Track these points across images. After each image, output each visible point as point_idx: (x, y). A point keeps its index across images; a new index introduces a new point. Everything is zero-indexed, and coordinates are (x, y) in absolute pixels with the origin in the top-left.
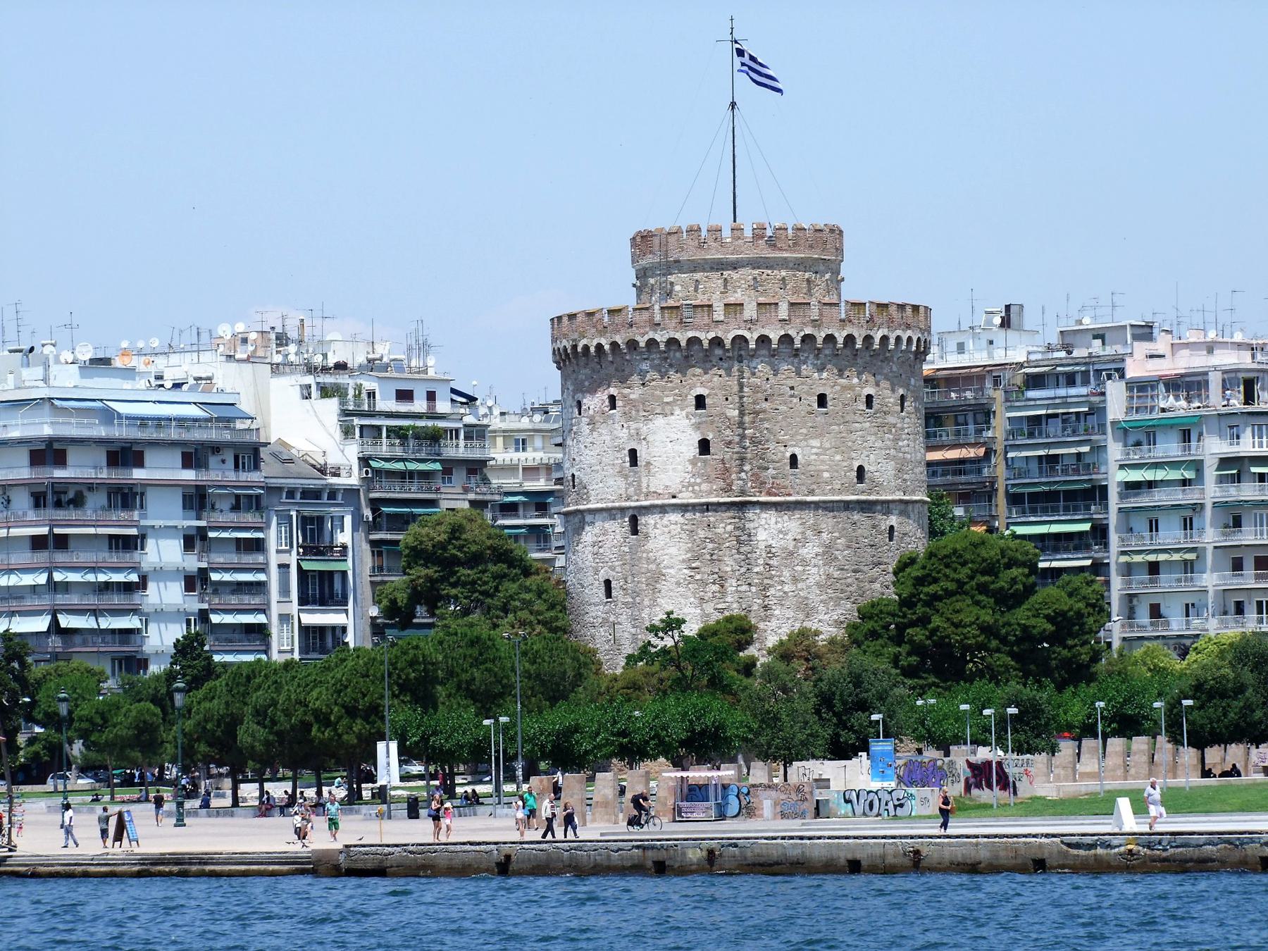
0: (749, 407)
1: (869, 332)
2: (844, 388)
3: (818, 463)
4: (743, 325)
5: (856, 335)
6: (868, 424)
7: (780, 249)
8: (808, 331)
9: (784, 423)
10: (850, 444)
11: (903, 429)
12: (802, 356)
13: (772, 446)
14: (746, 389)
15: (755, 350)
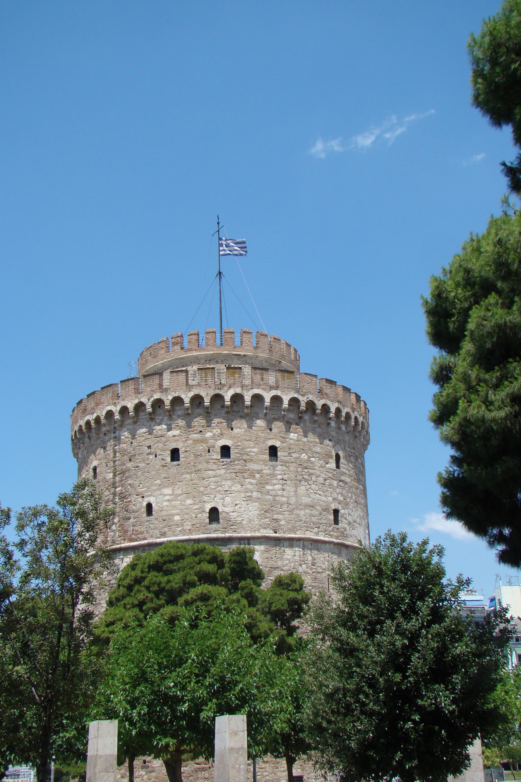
0: (119, 468)
1: (217, 392)
2: (196, 441)
3: (170, 508)
4: (111, 401)
5: (203, 394)
6: (223, 471)
7: (190, 350)
8: (157, 396)
9: (143, 478)
10: (202, 489)
11: (273, 475)
12: (158, 419)
13: (133, 498)
14: (118, 454)
15: (122, 421)
